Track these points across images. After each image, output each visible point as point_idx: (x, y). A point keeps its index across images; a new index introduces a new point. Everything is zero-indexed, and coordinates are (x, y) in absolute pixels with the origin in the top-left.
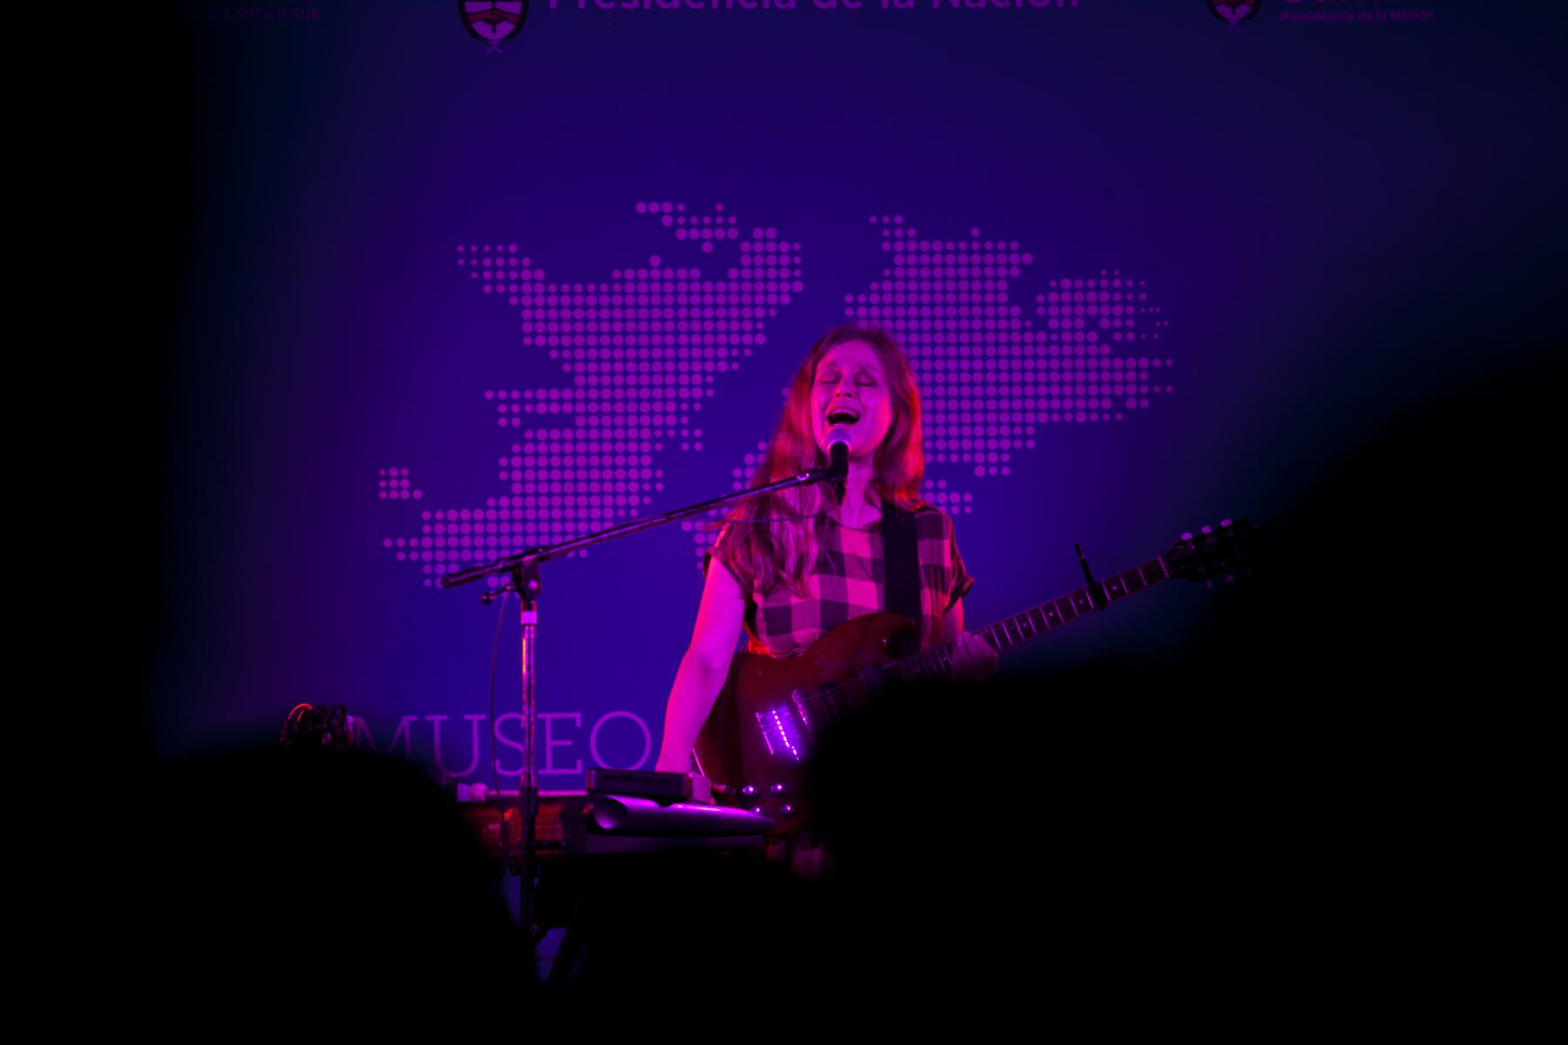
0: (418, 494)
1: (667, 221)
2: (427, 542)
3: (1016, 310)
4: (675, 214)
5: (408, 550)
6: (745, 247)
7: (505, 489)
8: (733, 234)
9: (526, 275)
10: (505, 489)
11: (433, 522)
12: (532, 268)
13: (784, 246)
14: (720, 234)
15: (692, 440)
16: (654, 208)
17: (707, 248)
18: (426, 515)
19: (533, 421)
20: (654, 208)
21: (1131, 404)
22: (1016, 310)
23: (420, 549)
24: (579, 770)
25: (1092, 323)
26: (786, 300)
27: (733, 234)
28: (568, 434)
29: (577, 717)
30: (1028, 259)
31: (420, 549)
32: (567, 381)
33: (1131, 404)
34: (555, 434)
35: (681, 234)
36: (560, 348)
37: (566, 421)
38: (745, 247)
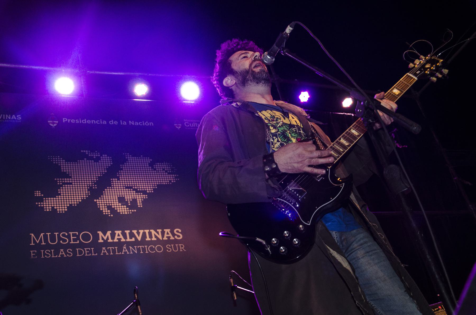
0: (42, 195)
1: (87, 153)
2: (45, 203)
3: (150, 167)
4: (88, 152)
5: (41, 204)
6: (101, 157)
7: (60, 194)
8: (99, 155)
9: (61, 161)
10: (60, 194)
11: (46, 200)
12: (62, 160)
13: (108, 157)
14: (97, 155)
15: (95, 187)
16: (84, 151)
17: (95, 157)
18: (44, 199)
19: (65, 184)
20: (84, 151)
21: (172, 181)
22: (150, 167)
23: (43, 204)
24: (78, 242)
25: (164, 169)
26: (110, 165)
27: (99, 155)
28: (71, 186)
29: (77, 233)
30: (151, 160)
31: (43, 204)
32: (71, 177)
33: (172, 181)
34: (69, 186)
35: (90, 155)
36: (69, 172)
37: (71, 184)
38: (101, 157)
